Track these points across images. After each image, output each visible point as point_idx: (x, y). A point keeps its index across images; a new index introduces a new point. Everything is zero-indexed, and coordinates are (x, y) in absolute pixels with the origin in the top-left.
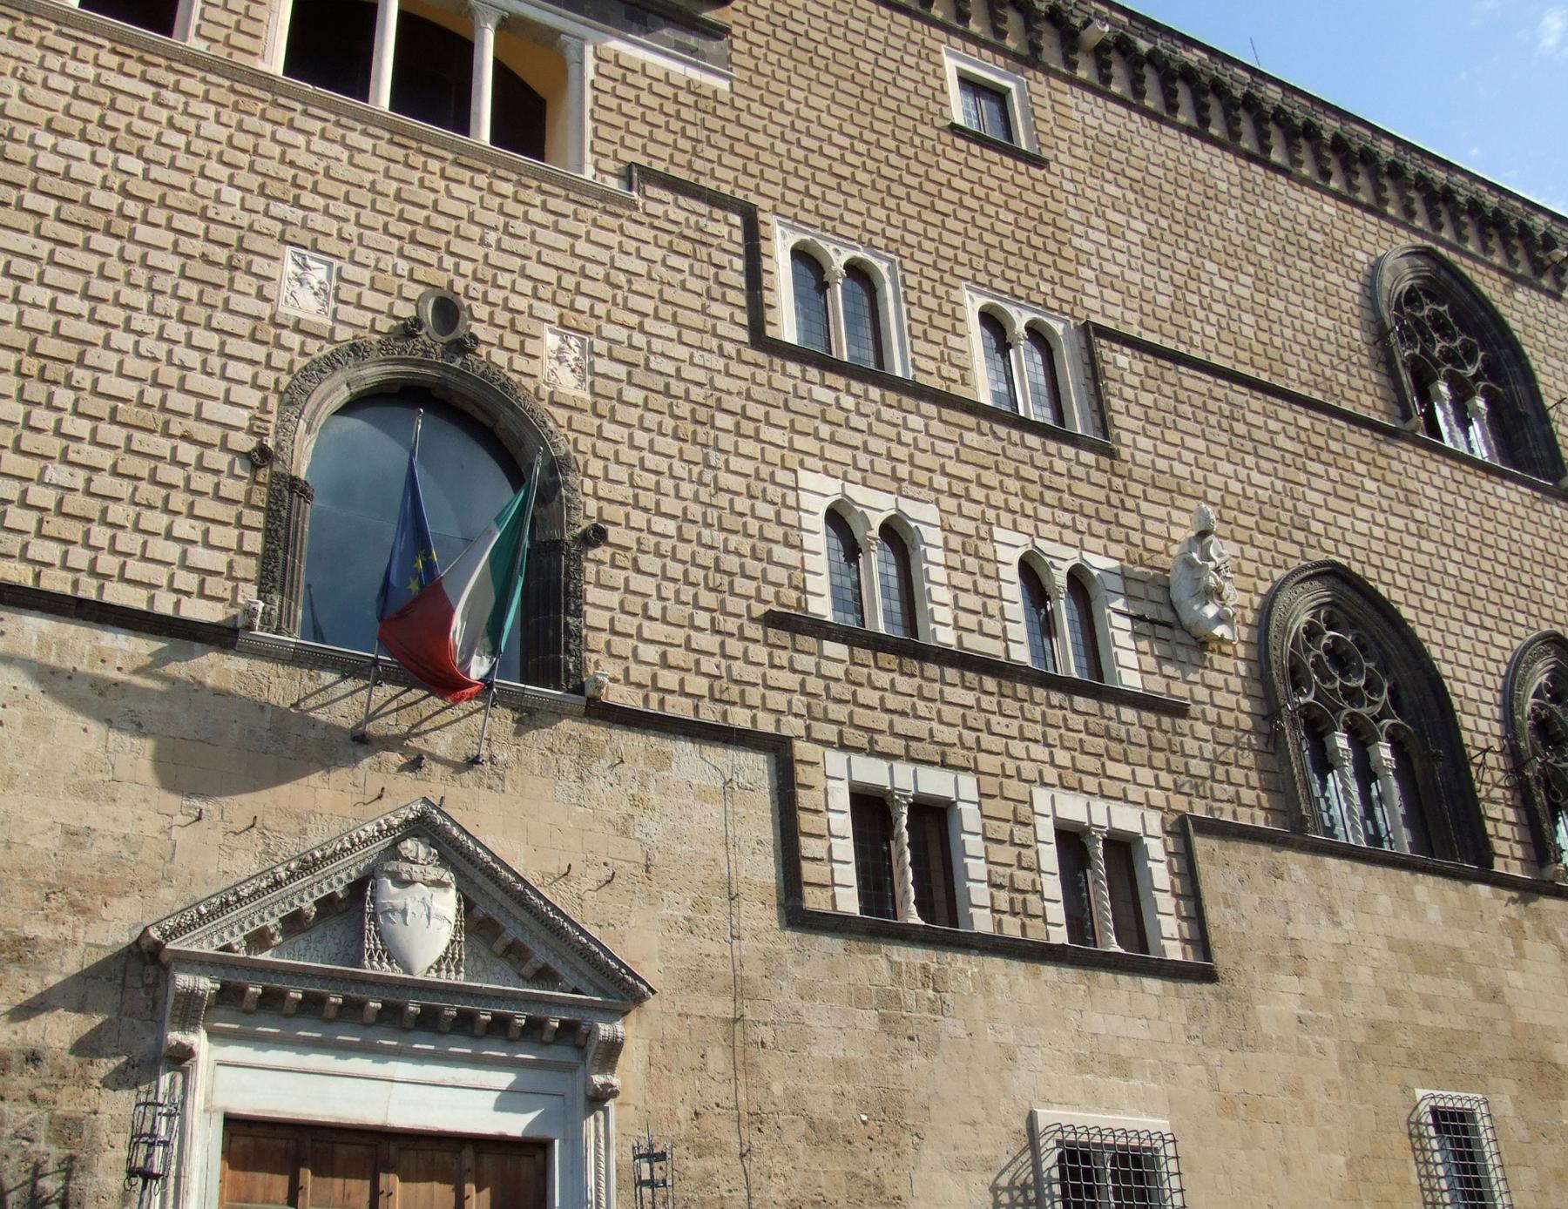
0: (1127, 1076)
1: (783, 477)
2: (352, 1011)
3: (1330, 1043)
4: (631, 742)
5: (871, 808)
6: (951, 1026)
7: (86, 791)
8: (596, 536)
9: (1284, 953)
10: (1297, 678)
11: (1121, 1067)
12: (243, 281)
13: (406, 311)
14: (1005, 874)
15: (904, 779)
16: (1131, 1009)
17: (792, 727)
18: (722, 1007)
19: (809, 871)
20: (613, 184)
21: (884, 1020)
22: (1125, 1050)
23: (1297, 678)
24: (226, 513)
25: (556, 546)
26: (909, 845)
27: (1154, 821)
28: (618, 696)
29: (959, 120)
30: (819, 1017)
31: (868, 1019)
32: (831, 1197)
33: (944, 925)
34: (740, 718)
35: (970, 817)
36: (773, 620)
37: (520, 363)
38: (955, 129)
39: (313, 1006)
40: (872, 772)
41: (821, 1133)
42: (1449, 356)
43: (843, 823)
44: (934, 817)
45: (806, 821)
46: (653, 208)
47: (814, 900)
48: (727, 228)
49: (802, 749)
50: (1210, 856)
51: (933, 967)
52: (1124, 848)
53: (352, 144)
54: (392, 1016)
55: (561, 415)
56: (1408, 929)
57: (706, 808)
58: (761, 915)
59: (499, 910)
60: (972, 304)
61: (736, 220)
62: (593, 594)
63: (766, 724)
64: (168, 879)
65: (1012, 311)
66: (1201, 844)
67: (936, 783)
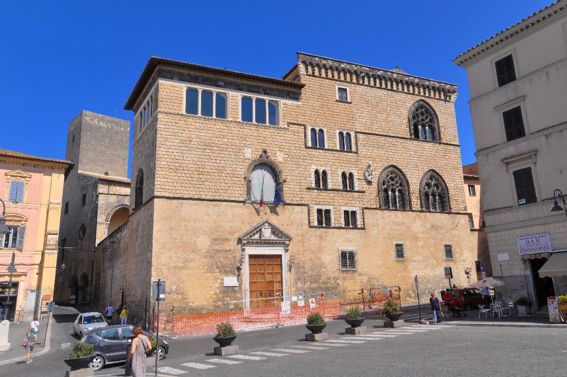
1: (309, 167)
2: (261, 243)
3: (381, 237)
4: (290, 207)
5: (319, 211)
7: (232, 222)
8: (285, 181)
9: (376, 225)
10: (384, 184)
11: (350, 241)
12: (240, 154)
13: (260, 154)
14: (337, 218)
15: (324, 208)
16: (352, 234)
17: (309, 203)
18: (300, 238)
19: (311, 221)
20: (286, 126)
21: (320, 238)
22: (351, 239)
23: (384, 184)
24: (242, 186)
25: (280, 184)
26: (324, 218)
27: (358, 209)
28: (288, 202)
29: (338, 99)
30: (312, 239)
31: (318, 238)
33: (328, 225)
34: (303, 202)
35: (332, 211)
36: (307, 188)
37: (276, 158)
38: (337, 101)
39: (257, 242)
40: (320, 207)
41: (313, 252)
42: (423, 120)
44: (328, 212)
46: (292, 129)
47: (312, 224)
48: (301, 129)
49: (311, 205)
52: (354, 213)
53: (252, 130)
54: (265, 243)
55: (279, 164)
56: (397, 220)
57: (300, 214)
58: (306, 227)
59: (275, 231)
60: (338, 132)
61: (303, 127)
62: (284, 189)
63: (306, 203)
64: (241, 230)
65: (343, 131)
66: (365, 210)
67: (328, 208)
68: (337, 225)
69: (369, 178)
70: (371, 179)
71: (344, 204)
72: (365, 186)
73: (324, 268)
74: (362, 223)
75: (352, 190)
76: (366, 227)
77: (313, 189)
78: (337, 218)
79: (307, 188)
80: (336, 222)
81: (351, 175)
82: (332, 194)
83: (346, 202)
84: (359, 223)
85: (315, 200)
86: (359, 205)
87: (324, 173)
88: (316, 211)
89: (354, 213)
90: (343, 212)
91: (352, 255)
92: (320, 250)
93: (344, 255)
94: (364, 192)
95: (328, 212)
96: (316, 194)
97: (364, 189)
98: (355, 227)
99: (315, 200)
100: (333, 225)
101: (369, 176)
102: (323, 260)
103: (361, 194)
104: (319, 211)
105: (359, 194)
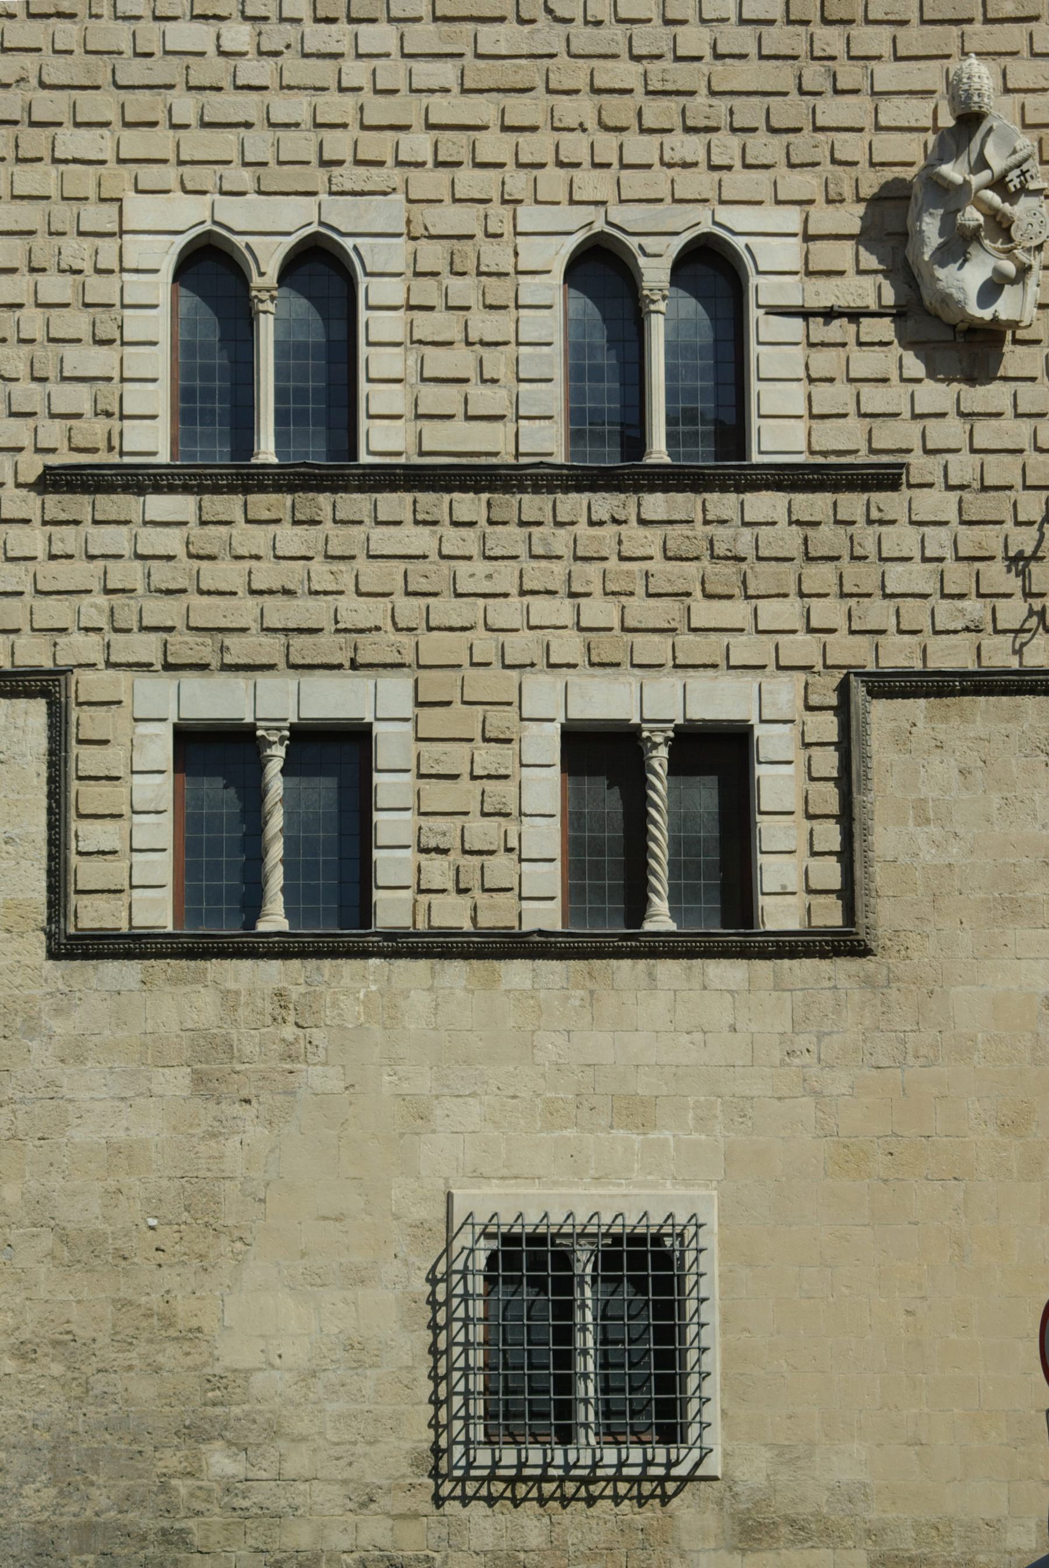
0: (644, 1127)
5: (210, 750)
6: (319, 1077)
11: (635, 1112)
14: (475, 818)
15: (275, 702)
16: (680, 1012)
21: (199, 1079)
27: (784, 694)
31: (175, 1082)
32: (83, 1334)
33: (341, 919)
35: (391, 746)
36: (54, 481)
41: (82, 1250)
43: (157, 789)
44: (338, 751)
45: (87, 796)
47: (92, 914)
49: (90, 684)
50: (902, 739)
51: (295, 993)
52: (719, 752)
66: (882, 716)
67: (331, 699)
68: (452, 914)
69: (965, 281)
70: (991, 290)
71: (568, 646)
72: (898, 396)
73: (240, 1447)
74: (829, 873)
75: (720, 450)
76: (885, 914)
77: (140, 480)
78: (475, 818)
79: (54, 481)
80: (438, 871)
81: (712, 268)
82: (398, 525)
83: (599, 611)
84: (787, 883)
85: (161, 611)
86: (802, 648)
87: (321, 267)
88: (159, 748)
89: (719, 752)
90: (545, 744)
91: (647, 1267)
92: (202, 1220)
93: (529, 1261)
94: (886, 477)
95: (338, 751)
96: (171, 541)
97: (887, 436)
98: (728, 920)
99: (161, 611)
100: (391, 910)
101: (958, 245)
102: (234, 1353)
103: (852, 504)
104: (210, 750)
105: (815, 504)
